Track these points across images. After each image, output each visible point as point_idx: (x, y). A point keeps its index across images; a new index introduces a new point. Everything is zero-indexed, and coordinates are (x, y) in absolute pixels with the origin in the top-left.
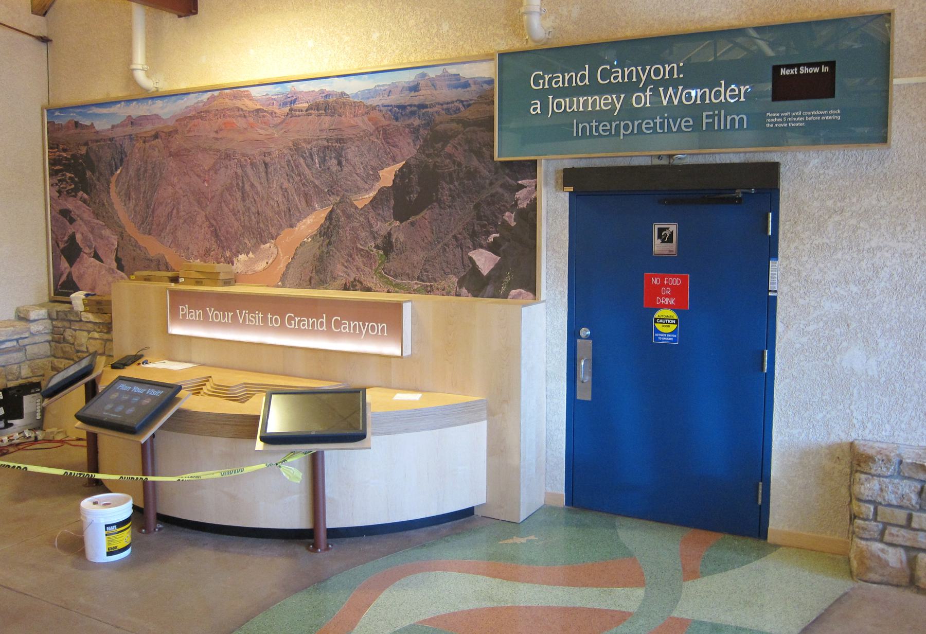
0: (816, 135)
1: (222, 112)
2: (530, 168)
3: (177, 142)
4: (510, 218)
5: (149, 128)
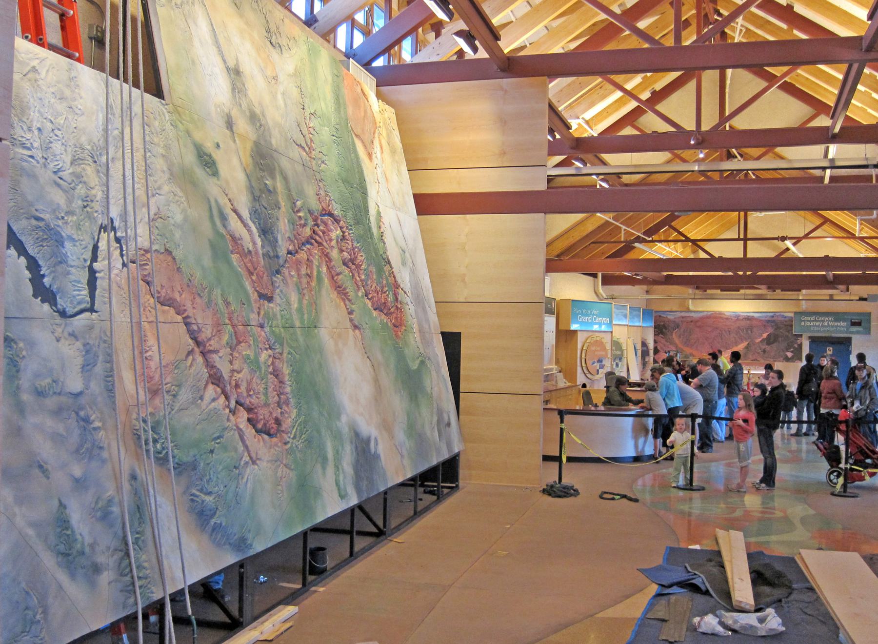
0: (858, 333)
1: (716, 318)
2: (801, 336)
3: (699, 324)
4: (796, 346)
5: (689, 319)
